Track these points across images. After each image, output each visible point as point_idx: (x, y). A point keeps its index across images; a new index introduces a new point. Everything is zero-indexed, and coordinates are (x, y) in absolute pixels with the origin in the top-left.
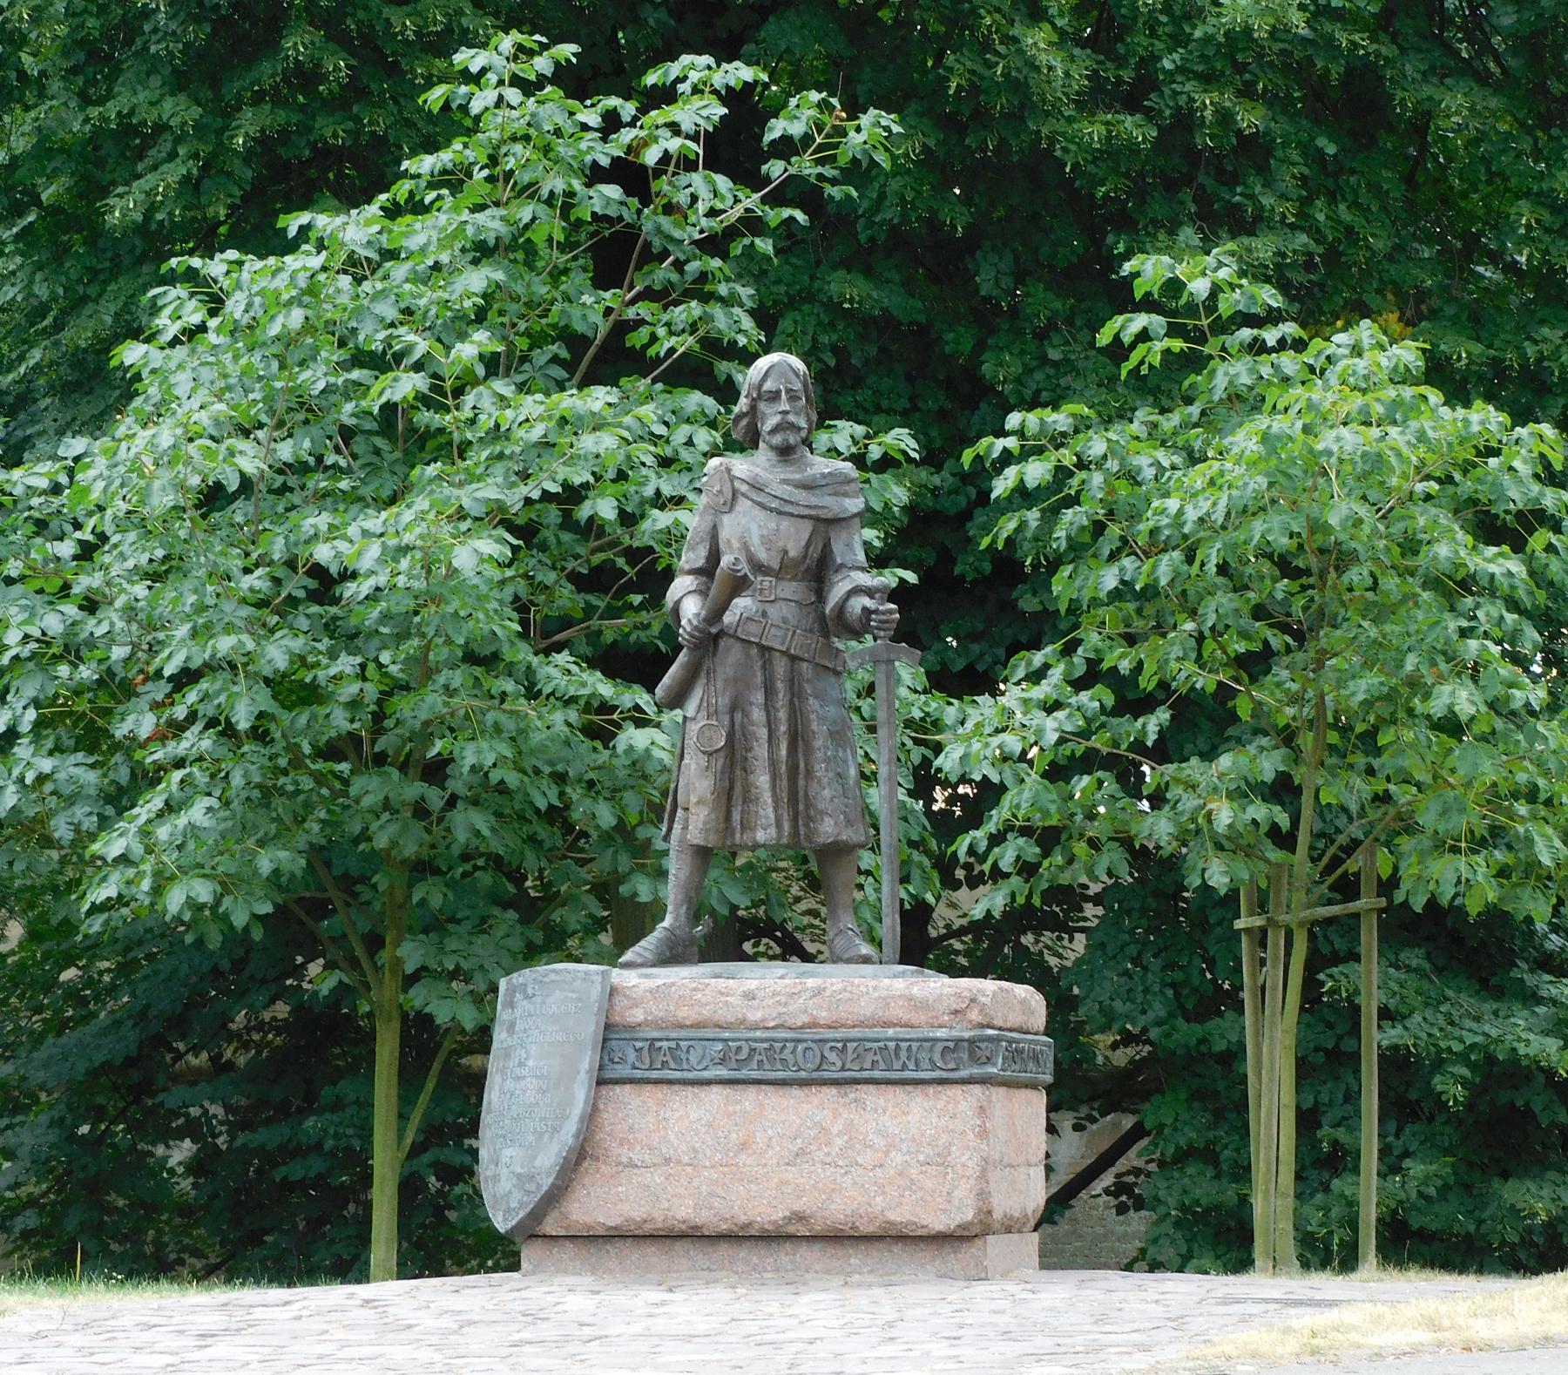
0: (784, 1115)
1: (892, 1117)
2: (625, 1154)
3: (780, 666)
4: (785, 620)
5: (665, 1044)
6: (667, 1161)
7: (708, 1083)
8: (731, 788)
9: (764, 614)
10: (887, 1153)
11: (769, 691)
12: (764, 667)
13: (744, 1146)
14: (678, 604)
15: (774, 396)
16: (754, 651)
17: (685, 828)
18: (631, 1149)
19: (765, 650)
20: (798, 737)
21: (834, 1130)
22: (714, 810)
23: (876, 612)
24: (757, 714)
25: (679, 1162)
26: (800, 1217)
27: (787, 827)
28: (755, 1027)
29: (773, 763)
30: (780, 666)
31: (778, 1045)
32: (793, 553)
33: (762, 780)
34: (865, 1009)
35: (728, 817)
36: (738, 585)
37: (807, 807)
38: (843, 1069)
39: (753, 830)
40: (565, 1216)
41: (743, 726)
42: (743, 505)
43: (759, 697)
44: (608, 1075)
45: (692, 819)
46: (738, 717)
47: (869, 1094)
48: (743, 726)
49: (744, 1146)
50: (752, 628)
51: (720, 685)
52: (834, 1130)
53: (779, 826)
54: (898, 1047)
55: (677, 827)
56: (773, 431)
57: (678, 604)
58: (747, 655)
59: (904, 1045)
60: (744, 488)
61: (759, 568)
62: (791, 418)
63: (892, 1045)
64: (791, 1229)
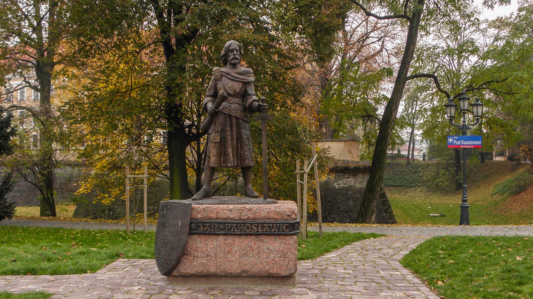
0: (239, 244)
1: (271, 244)
2: (196, 254)
3: (234, 120)
4: (235, 108)
5: (207, 224)
6: (208, 256)
7: (219, 235)
8: (221, 152)
9: (230, 106)
10: (269, 254)
11: (231, 127)
12: (230, 120)
13: (229, 252)
14: (206, 104)
15: (232, 51)
16: (227, 116)
17: (209, 162)
18: (198, 252)
19: (230, 116)
20: (240, 139)
21: (255, 248)
22: (216, 158)
23: (263, 106)
24: (229, 133)
25: (211, 256)
26: (244, 271)
27: (236, 162)
28: (232, 219)
29: (233, 145)
30: (234, 120)
31: (239, 225)
32: (237, 91)
33: (230, 150)
34: (263, 214)
35: (220, 160)
36: (224, 99)
37: (241, 157)
38: (257, 231)
39: (227, 163)
40: (179, 271)
41: (224, 136)
42: (224, 78)
43: (229, 129)
44: (192, 232)
45: (211, 160)
46: (223, 134)
47: (266, 239)
48: (224, 136)
49: (229, 252)
50: (227, 110)
51: (218, 125)
52: (255, 248)
53: (234, 163)
54: (273, 226)
55: (206, 162)
56: (232, 60)
57: (206, 104)
58: (226, 118)
59: (275, 225)
60: (224, 74)
61: (229, 95)
62: (236, 56)
63: (271, 225)
64: (242, 274)
